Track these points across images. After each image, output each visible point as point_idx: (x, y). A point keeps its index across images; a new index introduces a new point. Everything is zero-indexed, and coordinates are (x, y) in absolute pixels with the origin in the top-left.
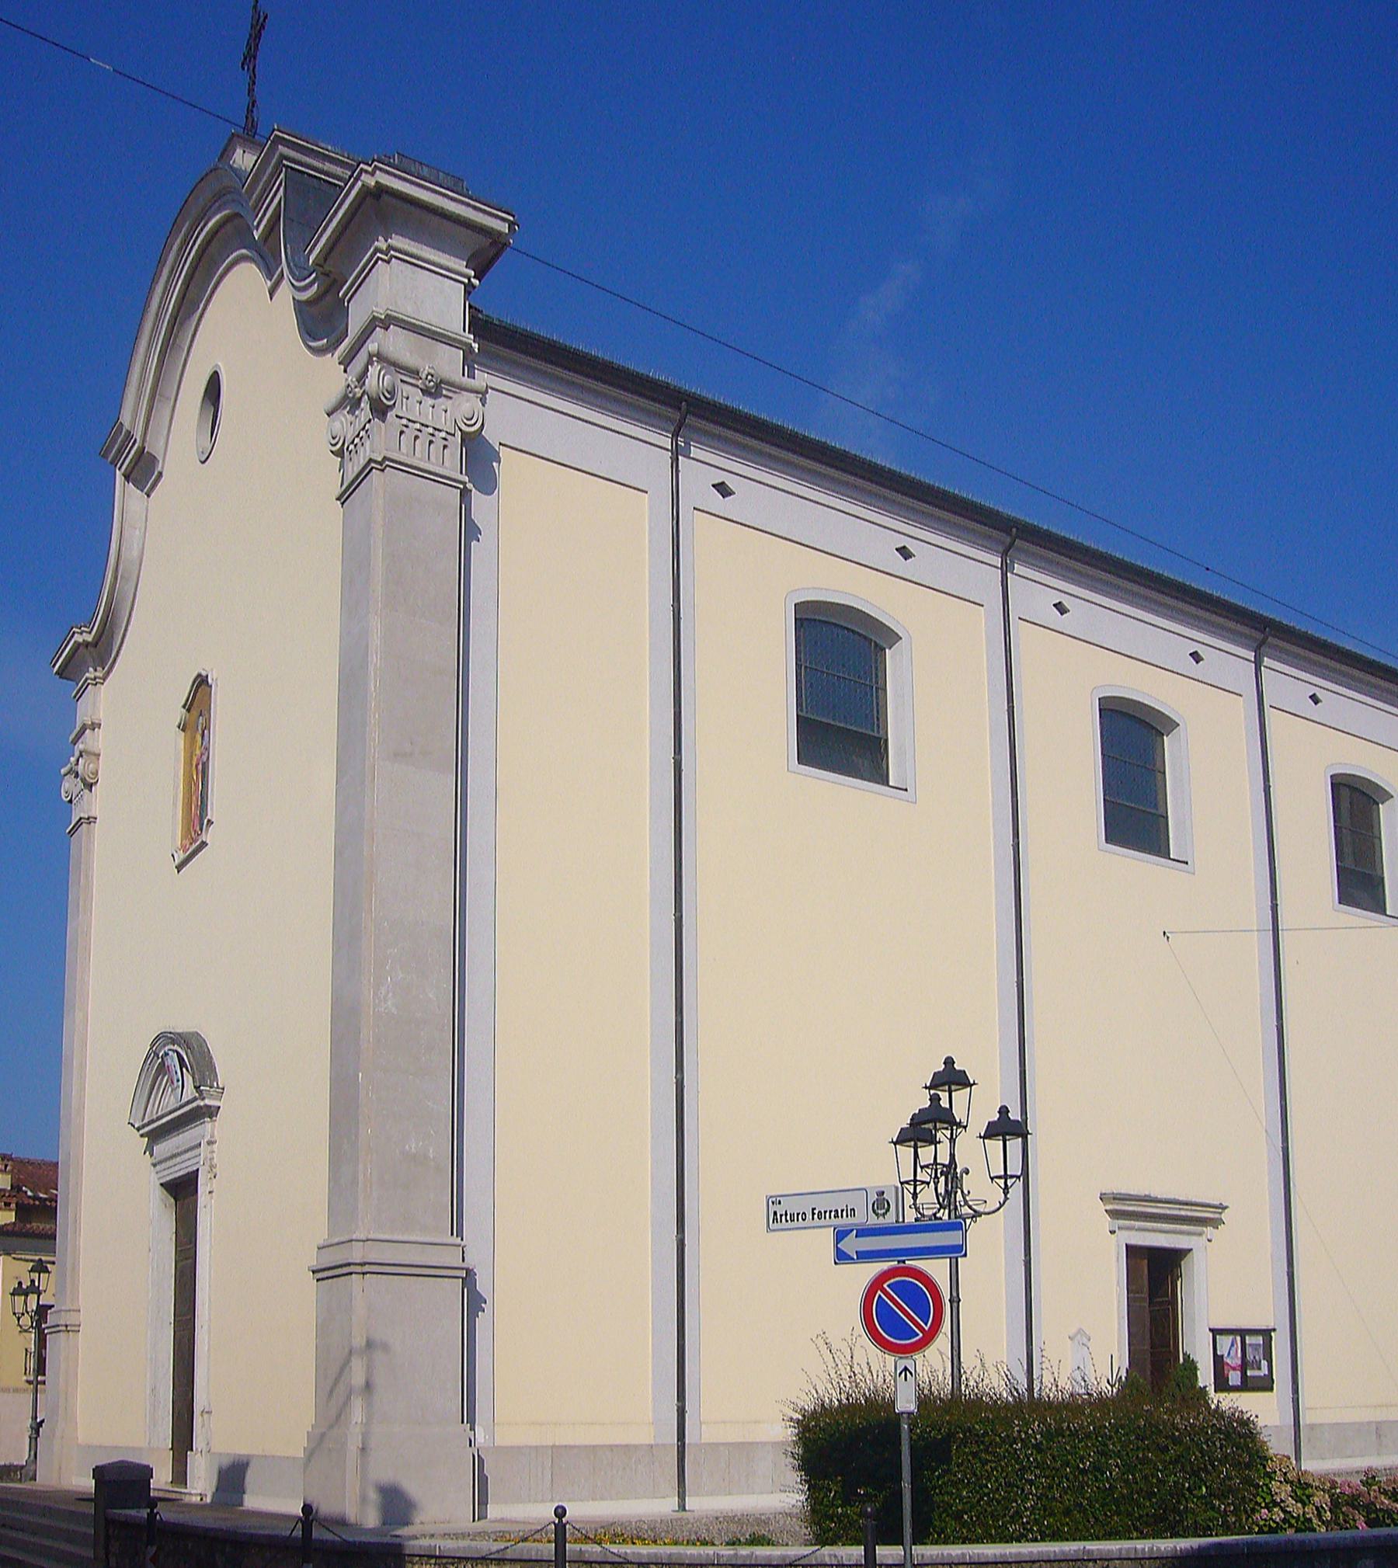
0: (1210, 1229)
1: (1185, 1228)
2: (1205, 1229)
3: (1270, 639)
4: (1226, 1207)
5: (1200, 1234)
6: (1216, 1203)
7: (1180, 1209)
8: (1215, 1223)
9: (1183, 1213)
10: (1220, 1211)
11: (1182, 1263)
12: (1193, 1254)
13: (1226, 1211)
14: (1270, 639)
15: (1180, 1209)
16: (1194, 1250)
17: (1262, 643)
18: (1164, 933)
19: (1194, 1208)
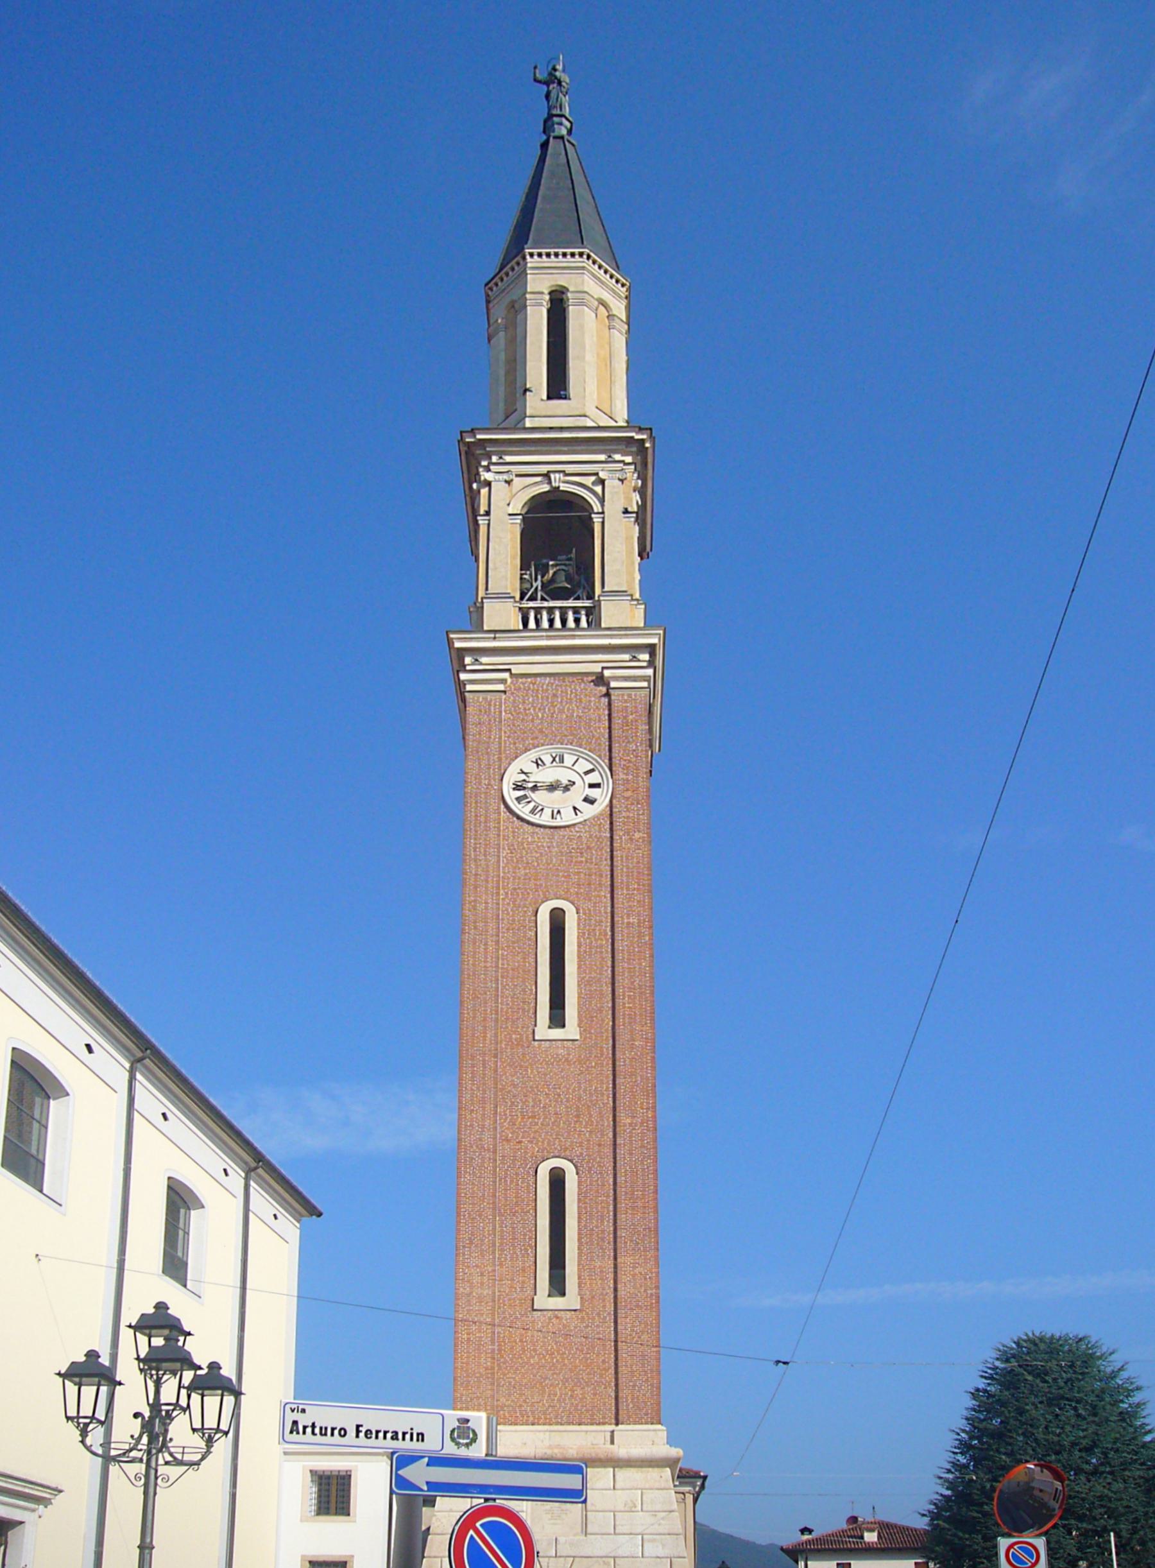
0: (41, 1507)
1: (22, 1503)
2: (37, 1506)
3: (147, 1061)
4: (61, 1491)
5: (33, 1510)
6: (54, 1485)
7: (25, 1487)
8: (45, 1502)
9: (27, 1491)
10: (56, 1493)
11: (9, 1533)
12: (24, 1527)
13: (61, 1494)
14: (147, 1061)
15: (25, 1487)
16: (27, 1525)
17: (140, 1060)
18: (37, 1255)
19: (37, 1487)
